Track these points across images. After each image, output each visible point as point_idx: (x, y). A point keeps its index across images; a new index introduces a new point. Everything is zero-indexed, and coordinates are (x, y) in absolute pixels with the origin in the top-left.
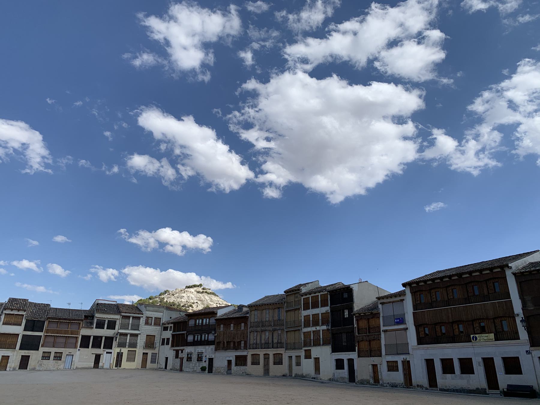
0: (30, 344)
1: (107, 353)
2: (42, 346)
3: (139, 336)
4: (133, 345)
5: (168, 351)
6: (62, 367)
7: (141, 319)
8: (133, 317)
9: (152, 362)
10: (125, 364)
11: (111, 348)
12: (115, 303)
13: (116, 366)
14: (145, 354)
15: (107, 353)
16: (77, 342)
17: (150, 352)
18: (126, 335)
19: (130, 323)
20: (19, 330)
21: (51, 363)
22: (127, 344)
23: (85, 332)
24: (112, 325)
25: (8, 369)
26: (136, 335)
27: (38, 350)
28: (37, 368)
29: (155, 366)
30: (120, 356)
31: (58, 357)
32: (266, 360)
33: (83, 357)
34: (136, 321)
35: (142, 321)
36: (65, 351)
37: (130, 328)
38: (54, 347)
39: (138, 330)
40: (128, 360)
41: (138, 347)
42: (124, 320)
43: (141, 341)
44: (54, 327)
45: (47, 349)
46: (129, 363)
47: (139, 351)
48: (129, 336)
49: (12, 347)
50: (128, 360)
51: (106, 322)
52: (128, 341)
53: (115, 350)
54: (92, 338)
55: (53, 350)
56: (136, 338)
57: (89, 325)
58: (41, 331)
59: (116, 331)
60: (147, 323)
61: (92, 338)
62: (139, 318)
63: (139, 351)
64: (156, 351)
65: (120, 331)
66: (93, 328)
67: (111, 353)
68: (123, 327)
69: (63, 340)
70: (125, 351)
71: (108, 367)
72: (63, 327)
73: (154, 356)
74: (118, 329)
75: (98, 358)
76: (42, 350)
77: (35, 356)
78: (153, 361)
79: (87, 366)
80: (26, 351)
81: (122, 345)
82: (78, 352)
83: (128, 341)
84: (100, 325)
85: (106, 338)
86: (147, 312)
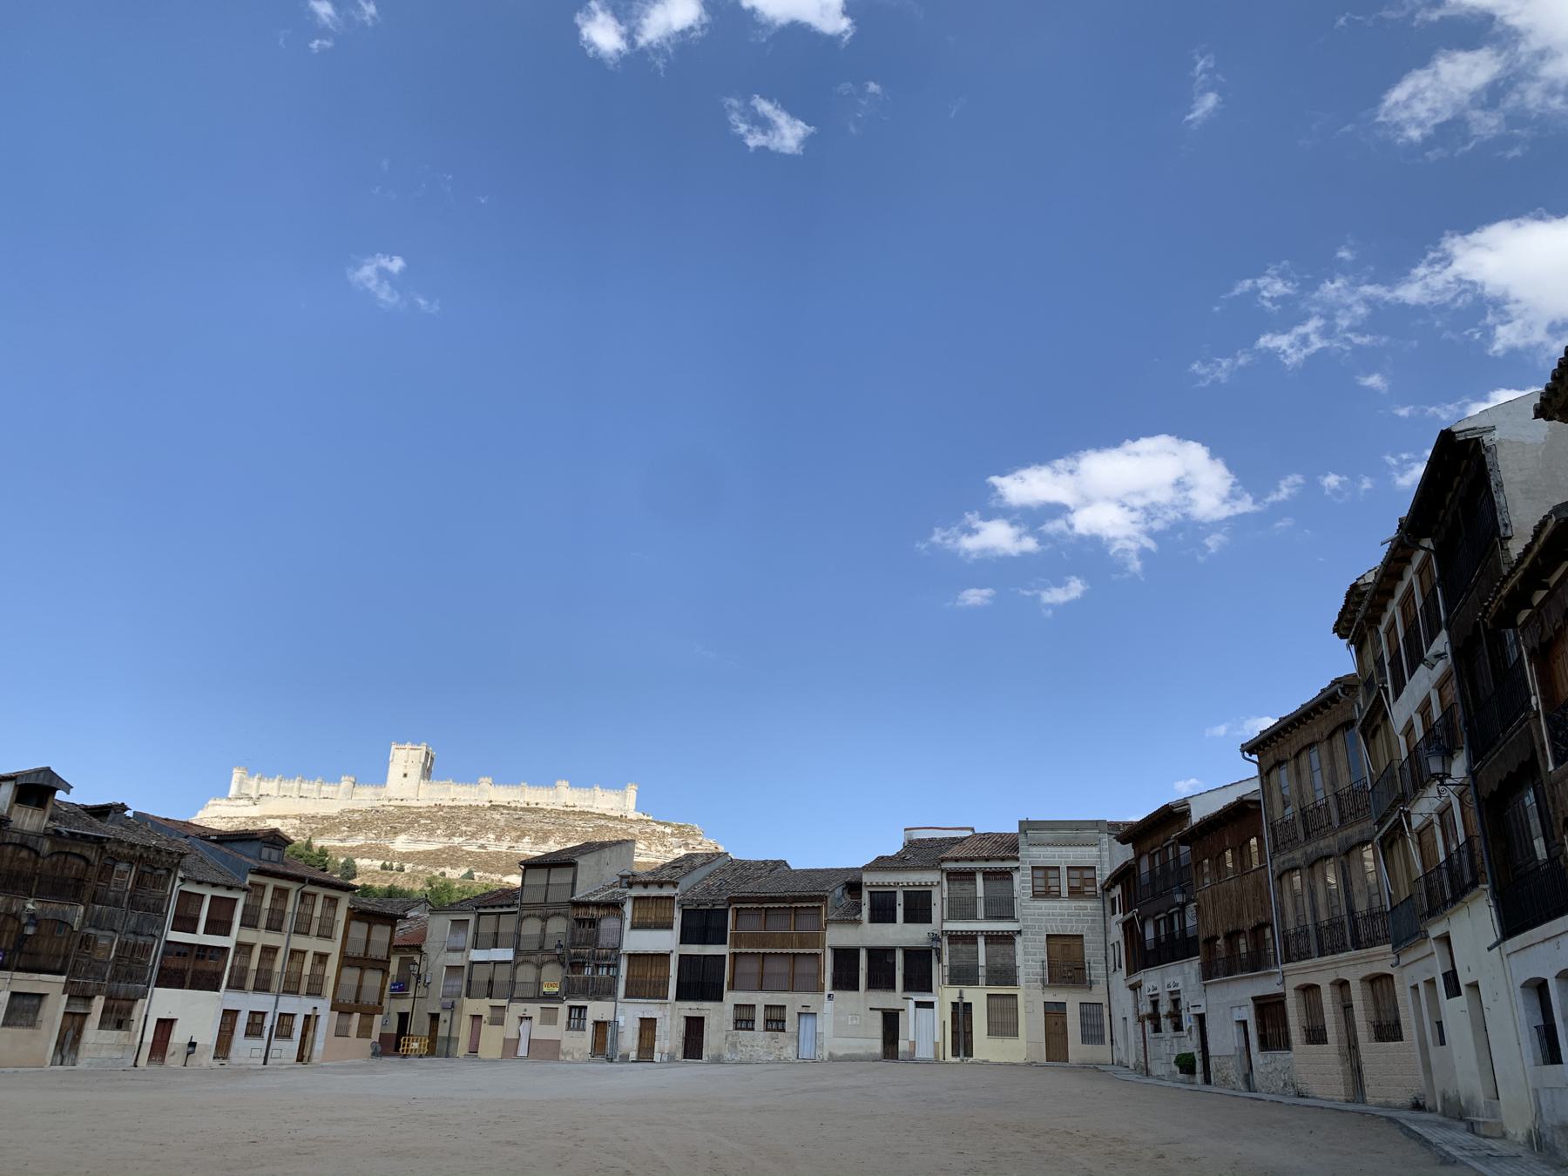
0: (700, 982)
1: (919, 1005)
2: (732, 987)
3: (1018, 939)
4: (1004, 974)
5: (1117, 994)
6: (789, 1052)
7: (1017, 877)
8: (987, 875)
9: (1086, 1038)
10: (984, 1045)
11: (930, 990)
12: (969, 833)
13: (955, 1053)
14: (1054, 1013)
15: (919, 1005)
16: (819, 973)
17: (1072, 1000)
18: (970, 938)
19: (980, 893)
20: (666, 941)
21: (758, 1040)
22: (982, 972)
23: (839, 936)
24: (918, 908)
25: (657, 1057)
26: (1008, 938)
27: (721, 999)
28: (727, 1056)
29: (1101, 1053)
30: (962, 1012)
31: (776, 1021)
32: (647, 1034)
33: (841, 1021)
34: (998, 886)
35: (1021, 883)
36: (793, 1002)
37: (981, 913)
38: (761, 989)
39: (1011, 917)
40: (995, 1030)
41: (1022, 979)
42: (957, 886)
43: (1030, 958)
44: (752, 925)
45: (743, 997)
46: (997, 1042)
47: (1030, 998)
48: (981, 941)
49: (658, 993)
50: (995, 1030)
51: (900, 899)
52: (982, 961)
53: (945, 995)
54: (863, 955)
55: (760, 999)
56: (1008, 948)
57: (850, 917)
58: (227, 933)
59: (934, 926)
60: (1045, 893)
61: (863, 955)
62: (1007, 875)
63: (1030, 998)
64: (1097, 995)
65: (949, 926)
66: (859, 922)
67: (930, 1005)
68: (962, 909)
69: (781, 967)
70: (977, 996)
71: (931, 1056)
72: (778, 926)
73: (1091, 1013)
74: (941, 922)
75: (891, 1021)
76: (731, 998)
77: (717, 1016)
78: (1093, 1034)
79: (861, 1052)
80: (693, 1004)
81: (963, 975)
82: (828, 1006)
83: (982, 961)
84: (883, 911)
85: (908, 952)
86: (1035, 851)
